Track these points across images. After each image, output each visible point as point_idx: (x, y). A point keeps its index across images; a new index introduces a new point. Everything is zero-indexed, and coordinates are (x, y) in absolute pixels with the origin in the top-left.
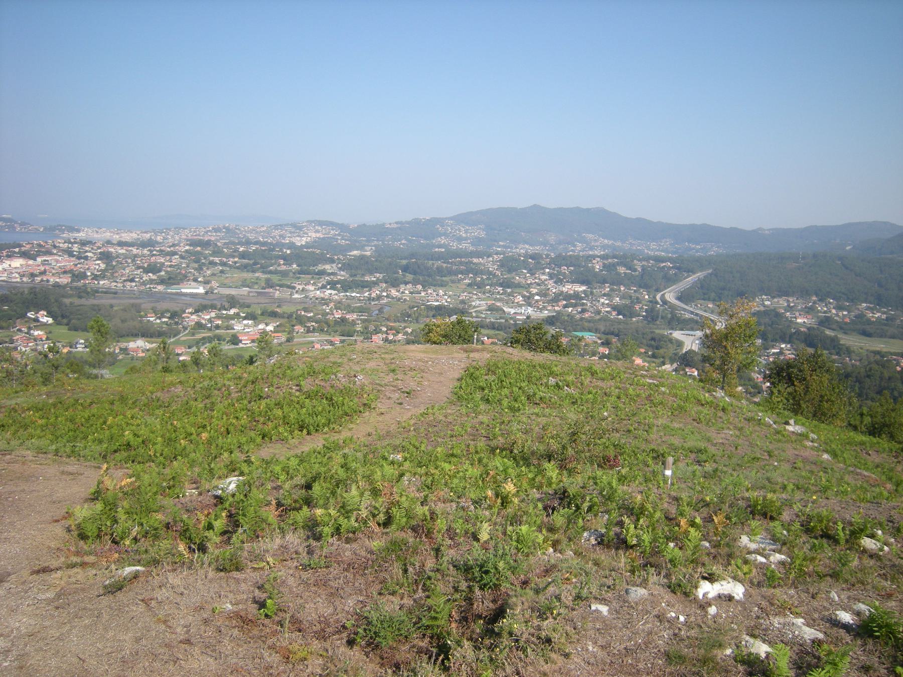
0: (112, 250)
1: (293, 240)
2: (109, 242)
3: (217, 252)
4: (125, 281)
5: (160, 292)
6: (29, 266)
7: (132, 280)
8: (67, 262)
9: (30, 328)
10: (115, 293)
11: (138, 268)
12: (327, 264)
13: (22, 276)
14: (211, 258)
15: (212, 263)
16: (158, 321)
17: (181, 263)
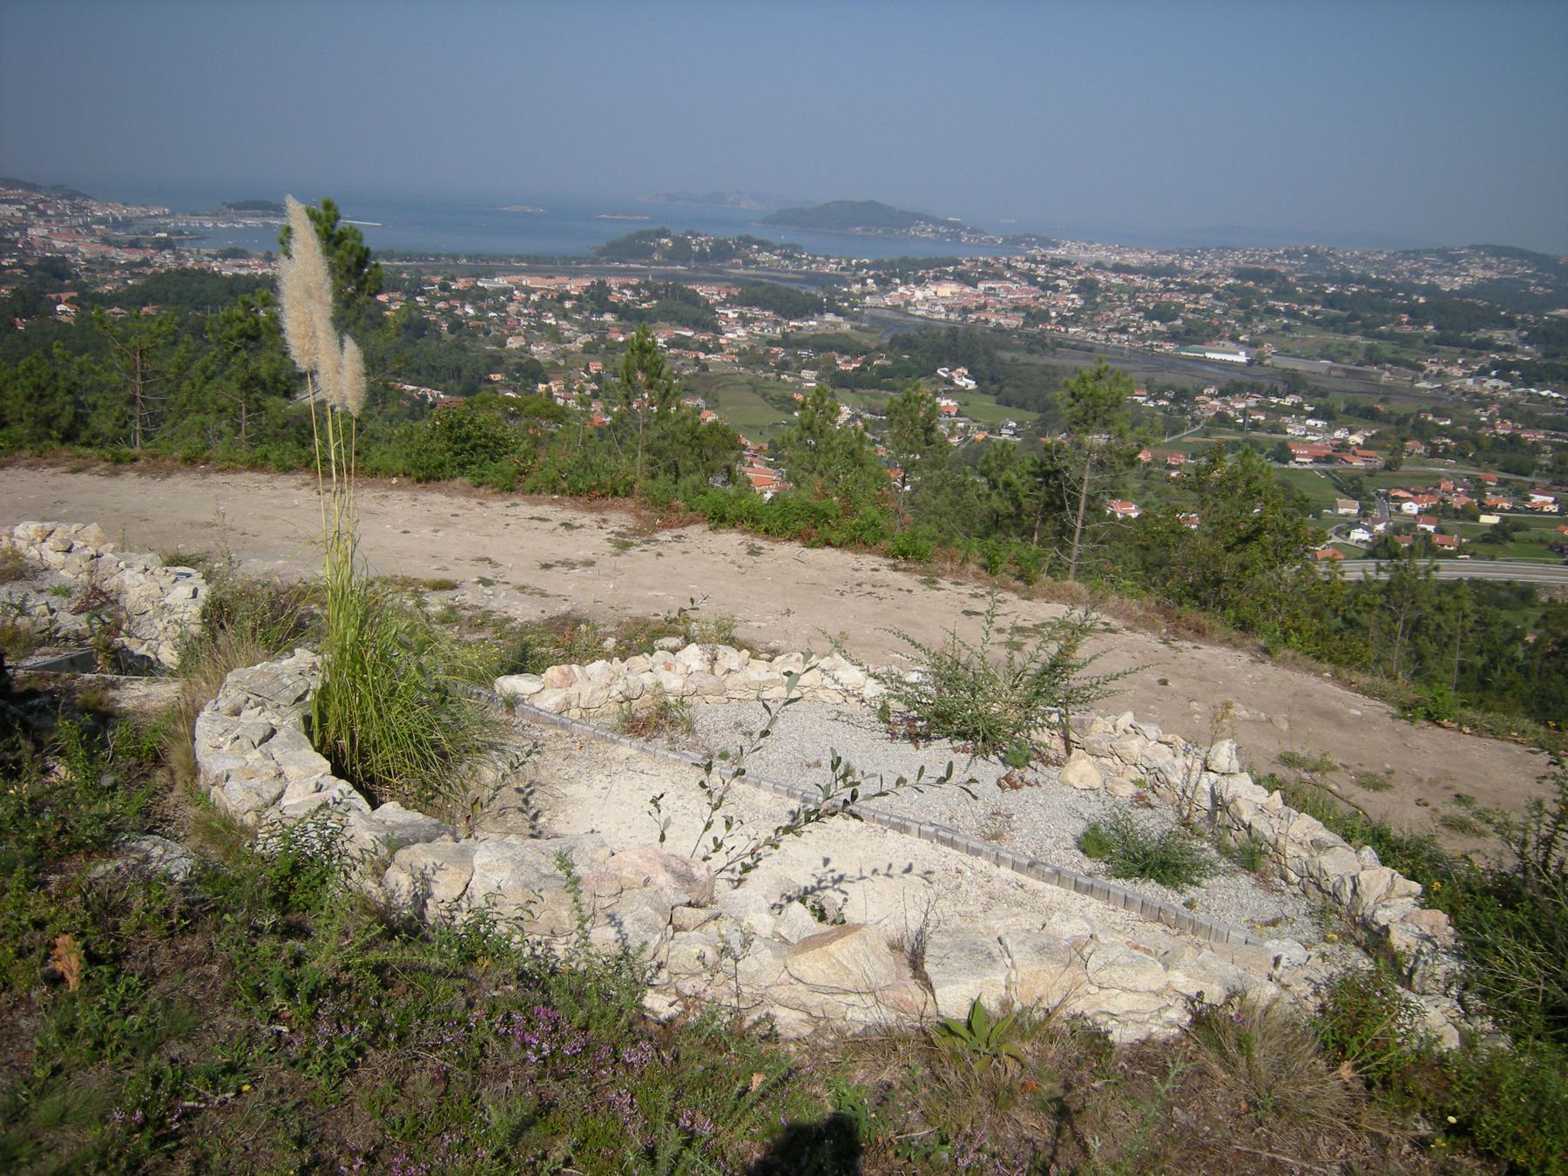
0: (1101, 277)
1: (1437, 280)
2: (1099, 265)
3: (1285, 292)
4: (1110, 330)
5: (1167, 355)
6: (965, 295)
7: (1123, 330)
8: (1020, 292)
9: (936, 394)
10: (1090, 350)
11: (1137, 310)
12: (1497, 328)
13: (949, 310)
14: (1271, 303)
15: (1272, 312)
16: (1151, 404)
17: (1215, 307)
